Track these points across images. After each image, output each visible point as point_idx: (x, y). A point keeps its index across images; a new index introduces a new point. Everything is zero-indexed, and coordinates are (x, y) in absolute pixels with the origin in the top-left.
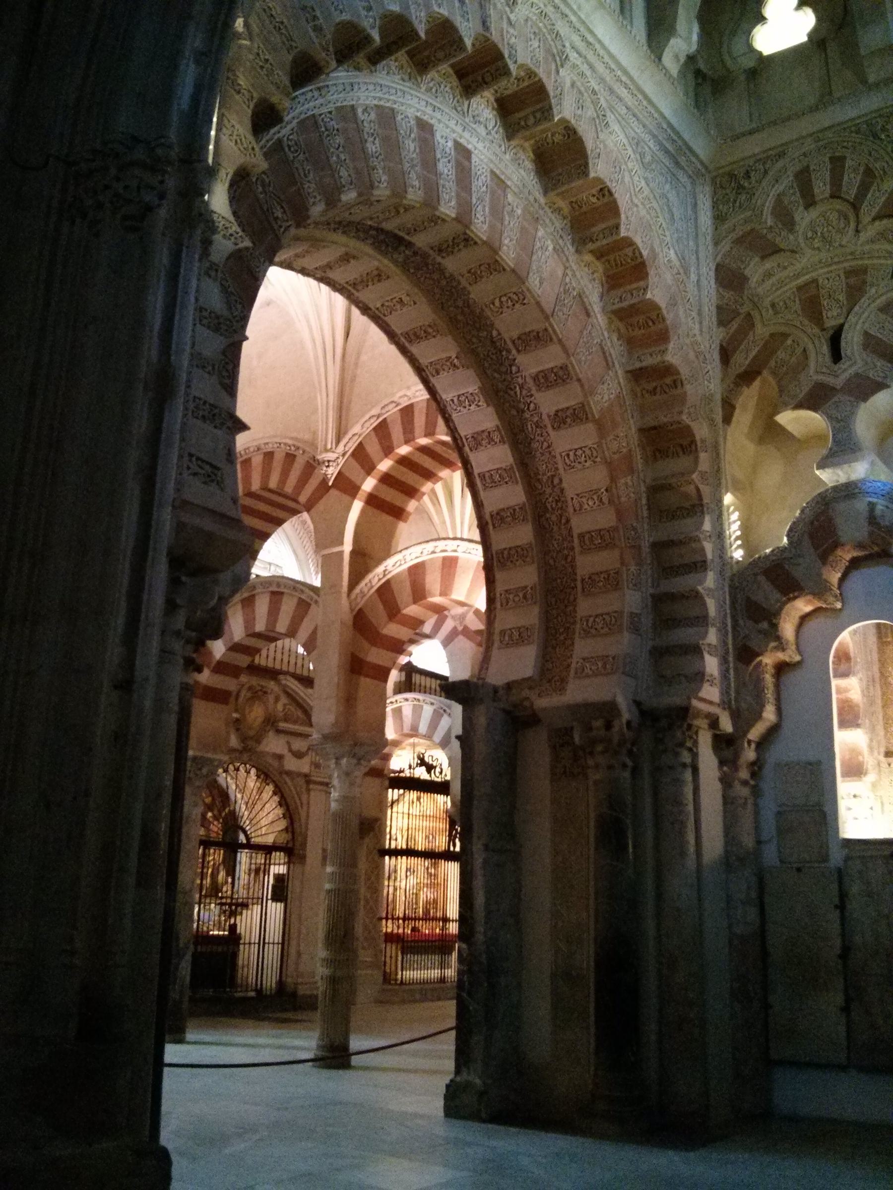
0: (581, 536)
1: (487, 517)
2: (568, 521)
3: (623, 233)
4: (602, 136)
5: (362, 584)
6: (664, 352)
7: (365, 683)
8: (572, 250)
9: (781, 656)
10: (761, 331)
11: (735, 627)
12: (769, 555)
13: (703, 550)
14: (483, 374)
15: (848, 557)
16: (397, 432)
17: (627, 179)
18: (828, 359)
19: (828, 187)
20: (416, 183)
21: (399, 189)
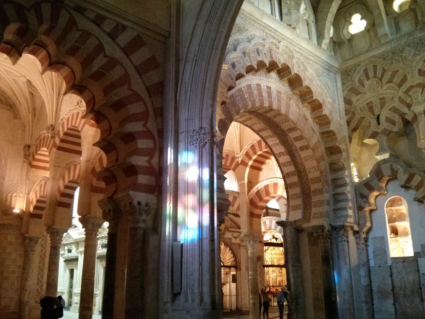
0: (311, 179)
1: (285, 175)
2: (307, 175)
3: (314, 98)
4: (306, 74)
5: (251, 191)
6: (329, 127)
7: (255, 219)
8: (301, 103)
9: (371, 208)
10: (357, 117)
11: (357, 201)
12: (365, 180)
13: (346, 181)
14: (279, 138)
15: (387, 179)
16: (257, 148)
17: (314, 82)
18: (376, 124)
19: (373, 74)
20: (258, 101)
21: (254, 102)
